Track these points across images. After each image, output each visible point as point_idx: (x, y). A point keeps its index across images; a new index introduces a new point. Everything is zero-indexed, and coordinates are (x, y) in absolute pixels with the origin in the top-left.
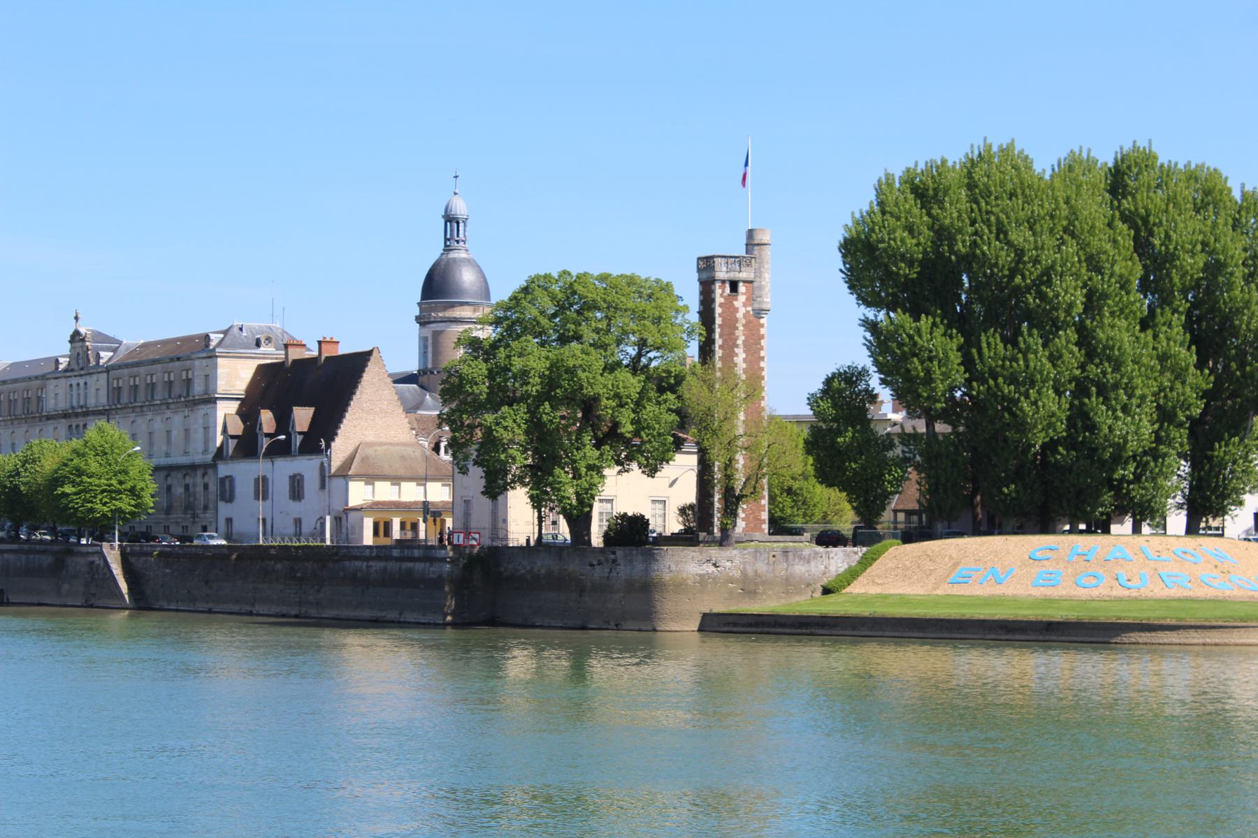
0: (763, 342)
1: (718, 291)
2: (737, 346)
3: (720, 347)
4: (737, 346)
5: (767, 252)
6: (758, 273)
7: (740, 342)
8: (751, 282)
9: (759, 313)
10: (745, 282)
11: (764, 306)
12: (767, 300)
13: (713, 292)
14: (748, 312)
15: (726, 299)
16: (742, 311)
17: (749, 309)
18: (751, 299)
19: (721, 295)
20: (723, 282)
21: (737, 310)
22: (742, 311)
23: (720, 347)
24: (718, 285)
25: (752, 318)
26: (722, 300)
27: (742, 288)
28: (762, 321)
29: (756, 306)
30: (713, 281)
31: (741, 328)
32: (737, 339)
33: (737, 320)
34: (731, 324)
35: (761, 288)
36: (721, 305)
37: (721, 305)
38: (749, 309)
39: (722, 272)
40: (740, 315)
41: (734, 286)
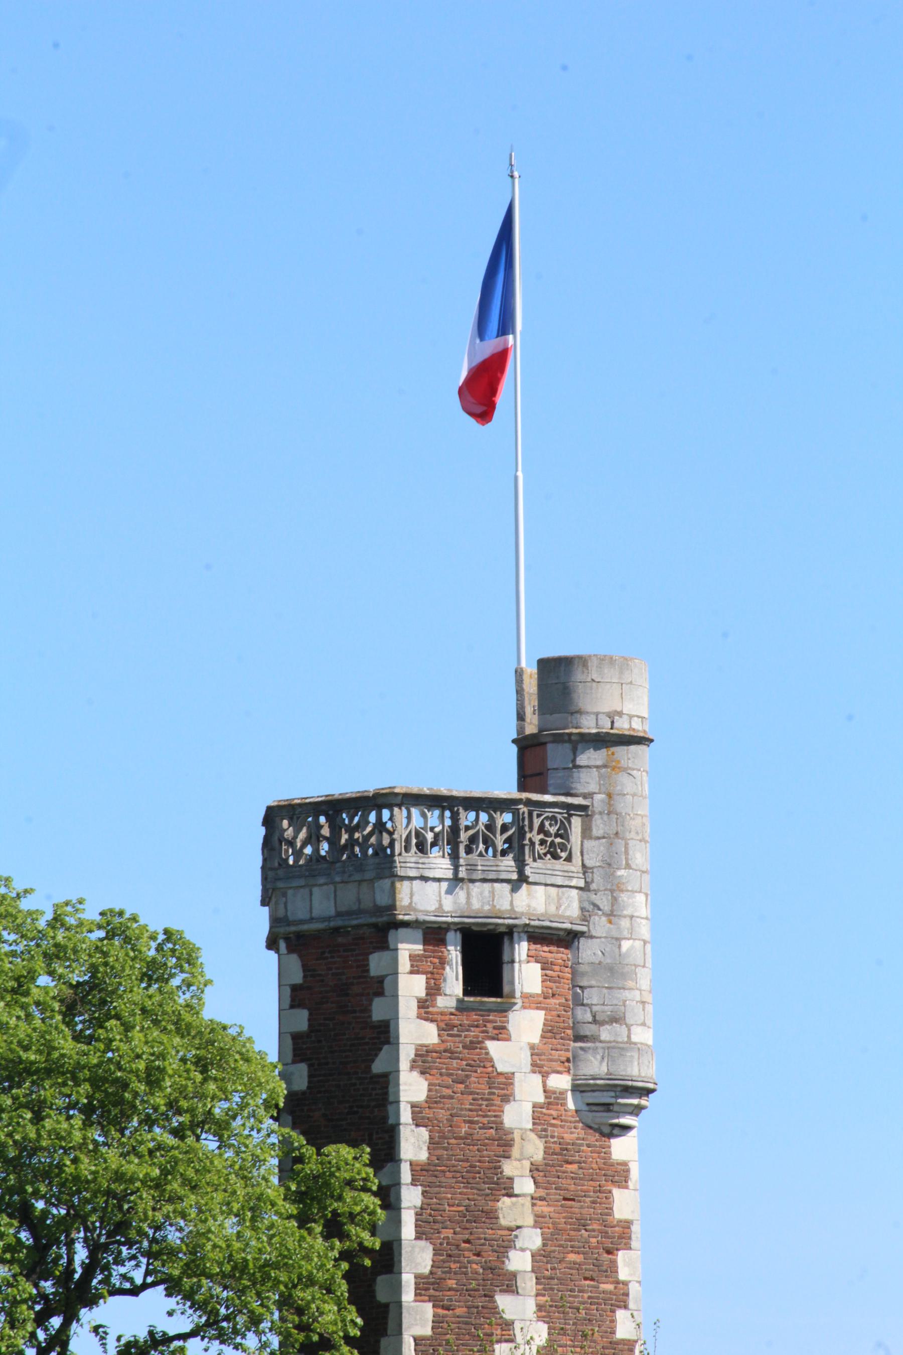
0: (627, 1265)
1: (411, 987)
2: (510, 1284)
3: (426, 1287)
4: (510, 1284)
5: (641, 783)
6: (602, 887)
7: (519, 1261)
8: (567, 939)
9: (609, 1104)
10: (541, 936)
11: (637, 1070)
12: (645, 1042)
13: (382, 987)
14: (553, 1098)
15: (446, 1028)
16: (529, 1090)
17: (561, 1082)
18: (569, 1034)
19: (425, 1007)
20: (434, 934)
21: (502, 1087)
22: (529, 1090)
23: (426, 1287)
24: (407, 949)
25: (574, 1134)
26: (430, 1034)
27: (526, 973)
28: (622, 1149)
29: (595, 1066)
30: (384, 927)
31: (525, 1186)
32: (505, 1245)
33: (504, 1143)
34: (472, 1165)
35: (615, 972)
36: (424, 1060)
37: (424, 1060)
38: (561, 1082)
39: (427, 891)
40: (517, 1115)
41: (485, 955)
